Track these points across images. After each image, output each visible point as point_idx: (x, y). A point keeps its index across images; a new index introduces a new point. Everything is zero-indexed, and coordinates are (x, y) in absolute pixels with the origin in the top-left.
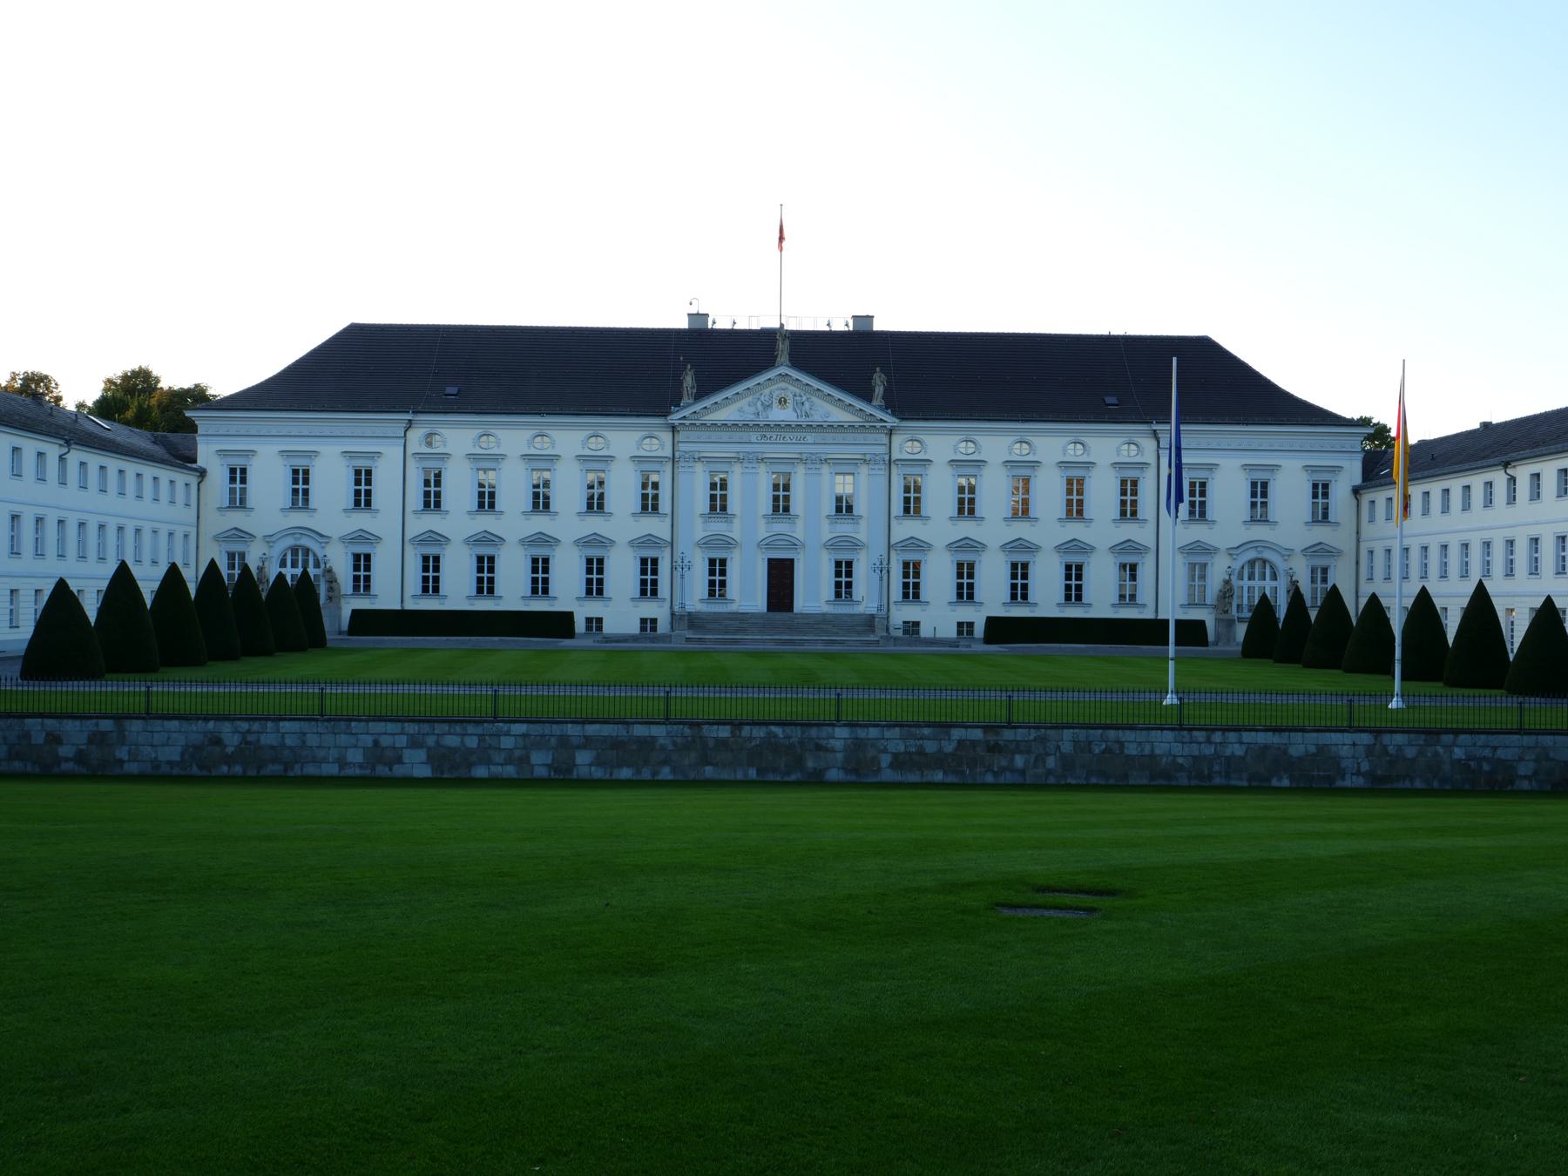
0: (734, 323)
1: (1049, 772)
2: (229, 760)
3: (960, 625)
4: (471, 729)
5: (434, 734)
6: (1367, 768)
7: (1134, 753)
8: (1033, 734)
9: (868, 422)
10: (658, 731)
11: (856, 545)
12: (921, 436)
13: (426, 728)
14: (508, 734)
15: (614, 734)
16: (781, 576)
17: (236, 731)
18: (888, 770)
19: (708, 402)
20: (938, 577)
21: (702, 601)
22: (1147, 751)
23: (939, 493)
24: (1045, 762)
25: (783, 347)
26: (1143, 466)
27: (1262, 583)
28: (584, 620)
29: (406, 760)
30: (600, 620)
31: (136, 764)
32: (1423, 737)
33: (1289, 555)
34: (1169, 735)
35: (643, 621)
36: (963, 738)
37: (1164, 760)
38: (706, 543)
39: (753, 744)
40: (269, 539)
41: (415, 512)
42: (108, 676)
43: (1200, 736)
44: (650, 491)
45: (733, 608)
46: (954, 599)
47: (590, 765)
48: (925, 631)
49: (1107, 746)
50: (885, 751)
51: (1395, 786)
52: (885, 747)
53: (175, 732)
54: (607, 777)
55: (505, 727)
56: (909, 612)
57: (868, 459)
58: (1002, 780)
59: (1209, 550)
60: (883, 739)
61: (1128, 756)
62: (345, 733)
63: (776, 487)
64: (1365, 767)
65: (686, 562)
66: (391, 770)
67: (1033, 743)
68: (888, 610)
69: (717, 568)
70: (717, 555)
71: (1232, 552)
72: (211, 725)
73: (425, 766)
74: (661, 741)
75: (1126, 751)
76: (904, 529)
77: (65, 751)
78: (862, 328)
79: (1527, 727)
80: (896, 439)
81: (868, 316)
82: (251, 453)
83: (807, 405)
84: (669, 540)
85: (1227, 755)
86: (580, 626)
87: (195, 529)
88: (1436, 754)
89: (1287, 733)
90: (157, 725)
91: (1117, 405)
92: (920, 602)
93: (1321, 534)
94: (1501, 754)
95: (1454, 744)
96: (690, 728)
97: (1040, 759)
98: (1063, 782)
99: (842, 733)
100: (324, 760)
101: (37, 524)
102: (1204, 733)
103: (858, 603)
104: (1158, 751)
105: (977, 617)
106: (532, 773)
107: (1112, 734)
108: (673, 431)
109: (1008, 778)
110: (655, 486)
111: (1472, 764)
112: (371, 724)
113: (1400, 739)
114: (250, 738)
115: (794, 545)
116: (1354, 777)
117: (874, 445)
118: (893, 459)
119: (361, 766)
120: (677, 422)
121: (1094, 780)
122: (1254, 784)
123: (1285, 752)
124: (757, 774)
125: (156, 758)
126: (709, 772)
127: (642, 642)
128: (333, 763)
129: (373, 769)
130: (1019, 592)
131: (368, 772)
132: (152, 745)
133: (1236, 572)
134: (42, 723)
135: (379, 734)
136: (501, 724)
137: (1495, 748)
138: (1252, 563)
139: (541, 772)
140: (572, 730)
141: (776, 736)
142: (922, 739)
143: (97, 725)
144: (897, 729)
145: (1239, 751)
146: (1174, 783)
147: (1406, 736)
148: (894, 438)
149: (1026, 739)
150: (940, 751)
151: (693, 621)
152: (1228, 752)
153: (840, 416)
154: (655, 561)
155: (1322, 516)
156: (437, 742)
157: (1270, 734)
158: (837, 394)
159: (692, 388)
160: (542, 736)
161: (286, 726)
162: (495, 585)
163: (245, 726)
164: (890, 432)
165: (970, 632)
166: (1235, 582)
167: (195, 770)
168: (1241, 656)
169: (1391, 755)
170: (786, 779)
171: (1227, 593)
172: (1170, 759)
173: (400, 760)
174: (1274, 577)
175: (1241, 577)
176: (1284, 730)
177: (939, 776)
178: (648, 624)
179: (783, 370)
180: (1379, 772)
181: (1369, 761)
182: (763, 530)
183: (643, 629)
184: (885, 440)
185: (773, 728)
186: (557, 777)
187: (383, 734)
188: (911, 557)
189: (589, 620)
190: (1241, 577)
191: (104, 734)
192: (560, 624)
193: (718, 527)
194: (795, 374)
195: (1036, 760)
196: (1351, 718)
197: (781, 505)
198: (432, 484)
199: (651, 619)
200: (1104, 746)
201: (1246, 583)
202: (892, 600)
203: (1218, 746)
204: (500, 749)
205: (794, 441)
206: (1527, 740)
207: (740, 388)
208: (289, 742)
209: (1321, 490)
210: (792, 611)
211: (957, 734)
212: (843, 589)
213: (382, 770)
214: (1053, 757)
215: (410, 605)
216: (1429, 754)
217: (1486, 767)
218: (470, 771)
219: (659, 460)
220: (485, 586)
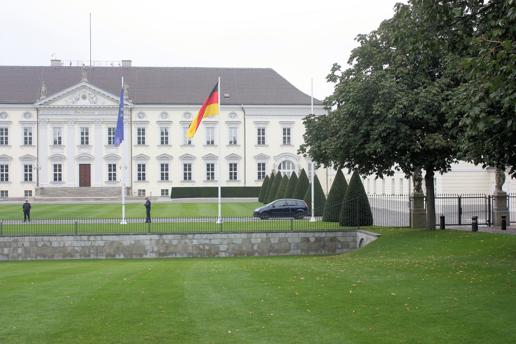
0: (71, 64)
1: (19, 255)
3: (163, 191)
6: (157, 249)
7: (57, 246)
8: (12, 239)
12: (167, 111)
19: (51, 98)
21: (51, 183)
22: (62, 245)
26: (238, 122)
27: (289, 171)
30: (7, 192)
32: (180, 235)
33: (299, 159)
34: (71, 238)
35: (26, 192)
37: (69, 248)
38: (52, 158)
43: (85, 238)
44: (28, 136)
46: (160, 179)
48: (147, 194)
49: (44, 243)
51: (168, 257)
56: (141, 186)
57: (67, 121)
61: (53, 247)
63: (82, 134)
64: (156, 249)
65: (39, 166)
67: (12, 243)
68: (132, 185)
69: (58, 168)
70: (58, 163)
71: (276, 158)
75: (53, 245)
78: (127, 65)
79: (224, 230)
80: (135, 113)
81: (129, 61)
83: (94, 98)
88: (186, 243)
89: (122, 236)
91: (229, 97)
92: (145, 181)
94: (213, 242)
95: (193, 239)
97: (15, 249)
98: (25, 259)
102: (86, 237)
103: (119, 182)
104: (66, 245)
105: (168, 186)
107: (46, 238)
108: (37, 110)
110: (30, 134)
111: (201, 246)
113: (170, 237)
115: (90, 158)
116: (151, 253)
118: (133, 121)
120: (38, 107)
121: (39, 258)
123: (121, 244)
127: (15, 201)
130: (187, 176)
137: (210, 239)
138: (284, 162)
145: (102, 244)
146: (73, 259)
148: (133, 112)
151: (43, 191)
152: (97, 245)
153: (109, 103)
154: (31, 166)
157: (115, 236)
158: (107, 94)
159: (45, 92)
162: (9, 177)
164: (131, 110)
165: (167, 194)
168: (258, 202)
169: (167, 244)
172: (72, 248)
174: (293, 167)
176: (121, 235)
178: (28, 193)
179: (84, 84)
180: (162, 251)
181: (157, 246)
182: (77, 152)
183: (26, 195)
188: (141, 162)
190: (280, 168)
193: (57, 151)
194: (89, 86)
195: (13, 250)
196: (292, 227)
197: (85, 141)
198: (28, 134)
200: (43, 243)
202: (133, 181)
203: (93, 242)
205: (89, 114)
206: (224, 236)
207: (65, 92)
210: (90, 185)
212: (112, 177)
214: (21, 248)
216: (183, 243)
217: (207, 248)
219: (31, 123)
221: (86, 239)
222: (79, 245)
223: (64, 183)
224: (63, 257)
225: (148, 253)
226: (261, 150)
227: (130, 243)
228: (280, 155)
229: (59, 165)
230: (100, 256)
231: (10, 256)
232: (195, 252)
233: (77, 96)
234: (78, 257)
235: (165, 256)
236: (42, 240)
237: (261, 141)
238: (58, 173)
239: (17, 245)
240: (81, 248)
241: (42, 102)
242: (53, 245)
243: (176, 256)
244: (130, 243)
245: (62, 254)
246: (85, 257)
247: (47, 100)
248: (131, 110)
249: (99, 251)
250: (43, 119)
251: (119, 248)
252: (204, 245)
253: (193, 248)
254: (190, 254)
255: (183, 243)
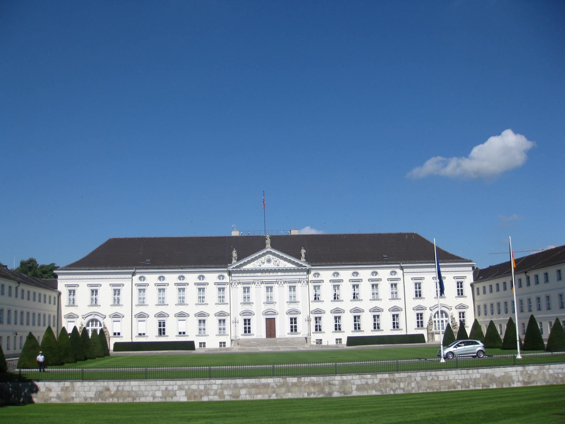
1: (413, 388)
2: (112, 396)
4: (201, 382)
5: (187, 385)
9: (300, 267)
10: (270, 380)
11: (297, 312)
13: (184, 382)
14: (215, 384)
15: (255, 382)
16: (271, 325)
17: (115, 386)
18: (355, 391)
19: (242, 262)
20: (328, 322)
22: (446, 379)
23: (327, 291)
24: (411, 385)
25: (268, 241)
27: (442, 319)
28: (199, 343)
29: (177, 395)
30: (204, 343)
31: (78, 398)
34: (454, 372)
35: (221, 343)
36: (382, 378)
37: (453, 381)
38: (243, 314)
39: (306, 384)
40: (84, 317)
41: (136, 305)
42: (48, 367)
43: (464, 371)
45: (254, 337)
47: (246, 394)
48: (324, 343)
49: (432, 378)
50: (354, 384)
52: (354, 383)
53: (93, 386)
54: (252, 399)
55: (213, 381)
56: (319, 336)
58: (396, 393)
59: (423, 308)
60: (353, 379)
61: (440, 381)
62: (155, 385)
64: (521, 379)
65: (237, 320)
66: (172, 398)
67: (407, 378)
69: (247, 322)
72: (106, 383)
73: (184, 397)
74: (272, 384)
75: (439, 379)
76: (315, 306)
77: (53, 394)
82: (78, 286)
83: (278, 261)
84: (230, 313)
85: (474, 378)
86: (197, 346)
87: (56, 314)
88: (544, 372)
90: (86, 383)
93: (461, 301)
95: (549, 369)
96: (282, 379)
97: (409, 384)
99: (338, 378)
100: (147, 396)
101: (8, 312)
104: (450, 378)
106: (224, 398)
107: (433, 373)
109: (399, 392)
111: (556, 375)
112: (164, 381)
114: (120, 389)
115: (275, 313)
116: (517, 383)
117: (302, 275)
118: (309, 280)
119: (161, 398)
120: (231, 270)
121: (429, 391)
122: (484, 388)
123: (494, 376)
124: (307, 395)
125: (86, 396)
126: (290, 396)
128: (151, 396)
129: (166, 398)
130: (357, 327)
131: (163, 400)
132: (84, 391)
133: (433, 316)
134: (44, 384)
135: (167, 385)
136: (212, 380)
137: (562, 369)
139: (227, 398)
140: (239, 381)
141: (314, 380)
142: (367, 379)
143: (64, 384)
144: (358, 375)
145: (478, 376)
146: (456, 390)
147: (533, 366)
149: (404, 377)
150: (373, 383)
152: (474, 377)
154: (224, 321)
155: (460, 293)
156: (189, 388)
158: (289, 258)
160: (228, 384)
161: (134, 383)
163: (117, 383)
164: (308, 272)
166: (433, 319)
167: (100, 401)
170: (318, 396)
171: (430, 323)
172: (455, 381)
173: (175, 395)
174: (447, 316)
175: (435, 317)
177: (374, 393)
178: (222, 344)
180: (526, 380)
182: (264, 308)
183: (221, 346)
184: (305, 273)
185: (313, 378)
186: (234, 399)
187: (169, 385)
189: (200, 343)
190: (435, 317)
191: (67, 387)
192: (190, 345)
193: (247, 307)
194: (273, 251)
195: (408, 385)
199: (223, 342)
200: (431, 378)
201: (437, 319)
204: (212, 390)
208: (134, 389)
209: (460, 285)
210: (275, 337)
211: (379, 376)
212: (294, 329)
213: (169, 400)
215: (135, 340)
217: (561, 376)
218: (201, 398)
219: (224, 284)
220: (162, 332)
221: (466, 373)
222: (460, 378)
223: (253, 335)
224: (449, 389)
225: (515, 383)
226: (419, 302)
227: (501, 375)
228: (435, 306)
229: (248, 320)
230: (477, 386)
231: (406, 389)
232: (551, 380)
233: (263, 260)
234: (459, 388)
235: (530, 384)
236: (431, 375)
237: (418, 295)
238: (247, 326)
239: (411, 380)
240: (462, 380)
241: (234, 266)
242: (439, 379)
243: (537, 384)
244: (501, 375)
245: (447, 386)
246: (466, 388)
247: (238, 264)
248: (308, 271)
249: (476, 382)
250: (235, 281)
251: (492, 379)
252: (558, 374)
253: (550, 377)
254: (548, 382)
255: (541, 373)
